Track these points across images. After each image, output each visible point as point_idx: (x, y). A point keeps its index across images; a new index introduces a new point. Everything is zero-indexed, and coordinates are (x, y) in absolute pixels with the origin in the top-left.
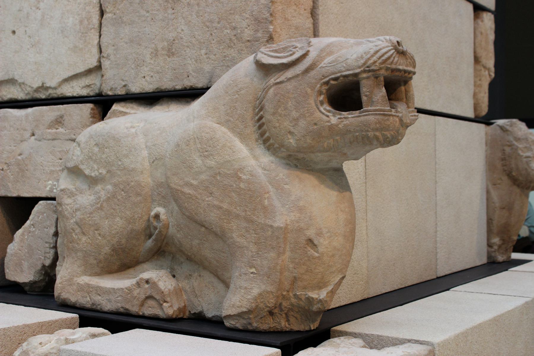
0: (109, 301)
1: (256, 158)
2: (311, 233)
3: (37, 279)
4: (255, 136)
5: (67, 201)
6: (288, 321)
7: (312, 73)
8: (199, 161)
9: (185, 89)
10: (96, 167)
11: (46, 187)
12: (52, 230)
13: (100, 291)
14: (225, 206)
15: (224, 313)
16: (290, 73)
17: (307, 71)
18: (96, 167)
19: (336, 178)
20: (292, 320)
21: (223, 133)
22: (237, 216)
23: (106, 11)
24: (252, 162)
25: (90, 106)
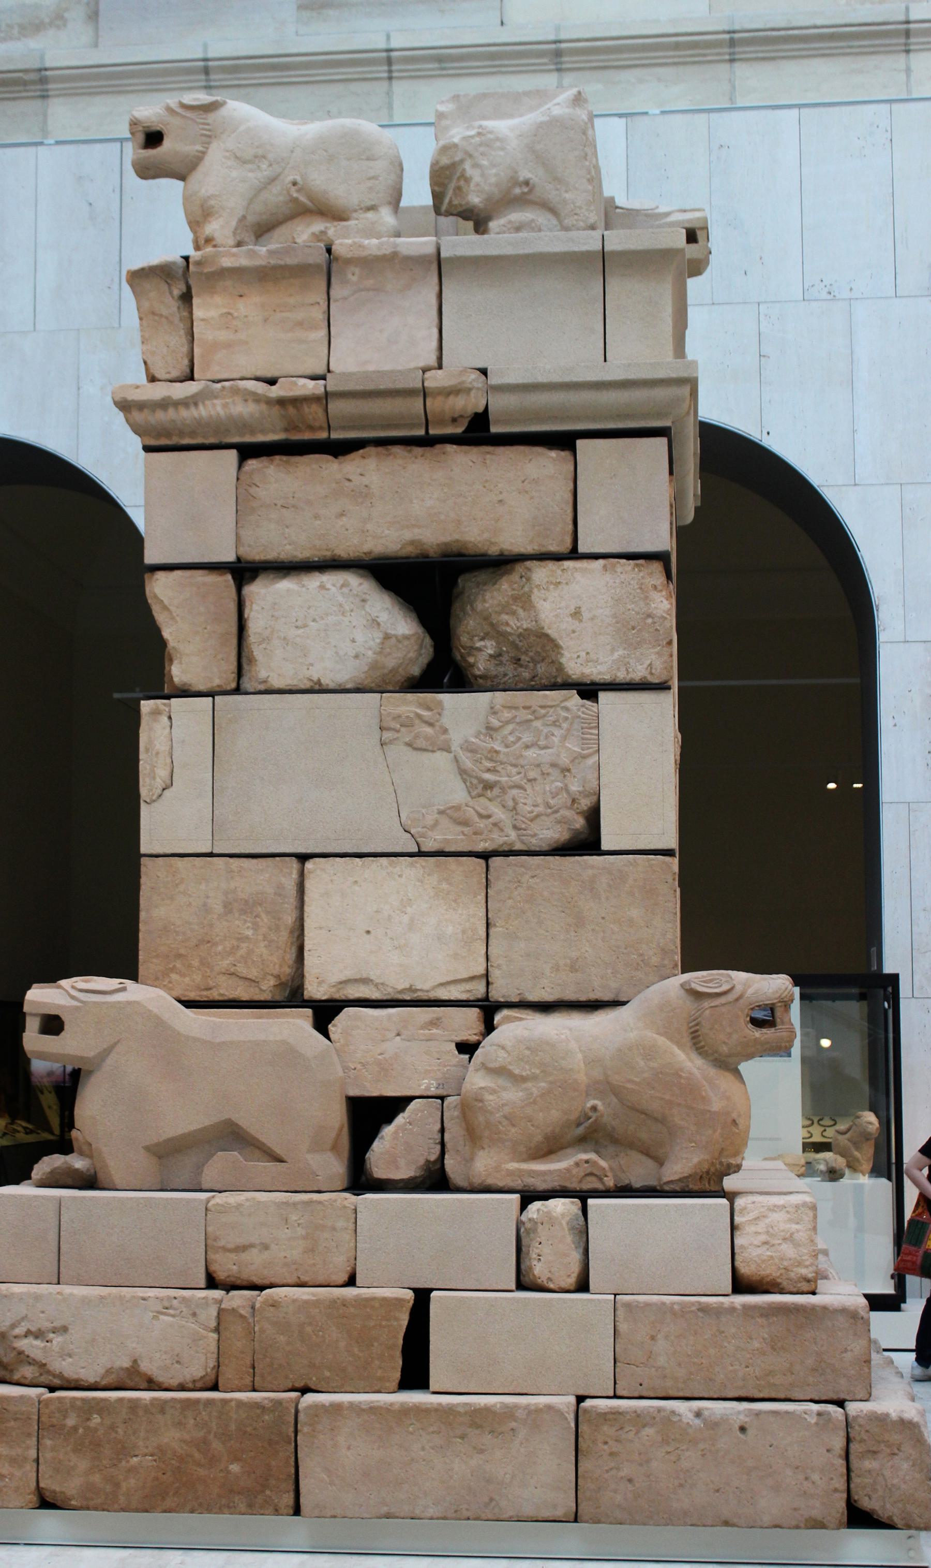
0: (545, 1181)
1: (690, 1060)
2: (734, 1115)
3: (418, 1175)
4: (689, 1044)
5: (488, 1097)
6: (709, 1183)
7: (741, 1001)
8: (642, 1063)
9: (590, 1001)
10: (527, 1067)
11: (420, 1086)
12: (438, 1126)
13: (532, 1173)
14: (667, 1097)
15: (665, 1179)
16: (722, 1000)
17: (737, 1000)
18: (527, 1067)
19: (737, 1073)
20: (712, 1182)
21: (662, 1041)
22: (679, 1105)
23: (495, 925)
24: (689, 1064)
25: (476, 1010)
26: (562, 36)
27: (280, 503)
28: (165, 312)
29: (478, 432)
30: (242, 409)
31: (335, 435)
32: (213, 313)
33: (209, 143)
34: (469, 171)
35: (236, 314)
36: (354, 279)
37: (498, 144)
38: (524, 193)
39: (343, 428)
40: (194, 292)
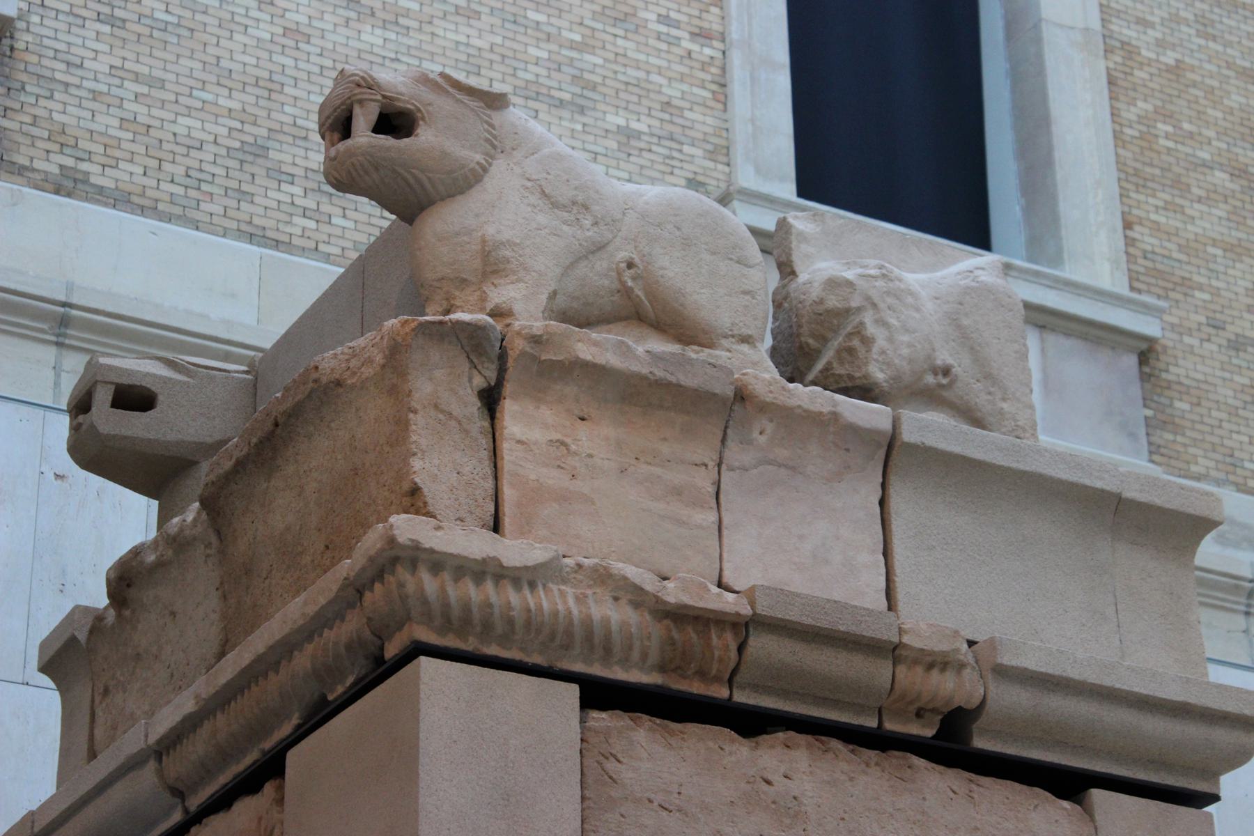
26: (75, 300)
27: (659, 798)
28: (456, 411)
29: (951, 742)
30: (609, 612)
31: (741, 697)
32: (537, 435)
33: (492, 158)
34: (871, 329)
35: (573, 447)
36: (762, 439)
37: (910, 300)
38: (941, 386)
39: (756, 688)
40: (508, 388)
